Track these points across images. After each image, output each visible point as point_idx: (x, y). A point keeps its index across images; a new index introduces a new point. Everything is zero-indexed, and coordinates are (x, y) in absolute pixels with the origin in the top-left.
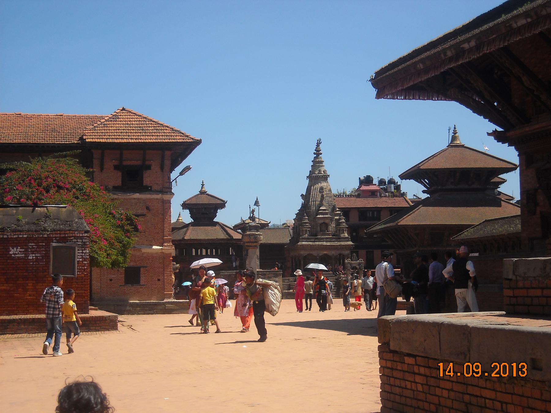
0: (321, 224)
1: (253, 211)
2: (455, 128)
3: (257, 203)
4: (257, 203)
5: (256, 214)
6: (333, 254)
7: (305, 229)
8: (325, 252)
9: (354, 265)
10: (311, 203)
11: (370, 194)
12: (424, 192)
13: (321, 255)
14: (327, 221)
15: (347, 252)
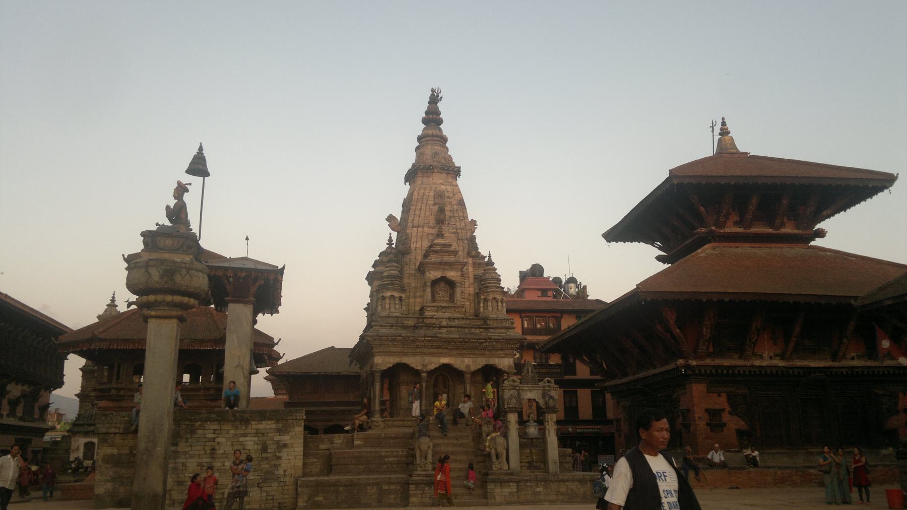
0: (435, 283)
1: (181, 190)
2: (724, 124)
3: (198, 167)
4: (198, 167)
5: (191, 200)
6: (468, 366)
7: (388, 294)
8: (445, 360)
9: (530, 395)
10: (413, 232)
11: (539, 293)
12: (659, 258)
13: (432, 367)
14: (452, 274)
15: (505, 363)
